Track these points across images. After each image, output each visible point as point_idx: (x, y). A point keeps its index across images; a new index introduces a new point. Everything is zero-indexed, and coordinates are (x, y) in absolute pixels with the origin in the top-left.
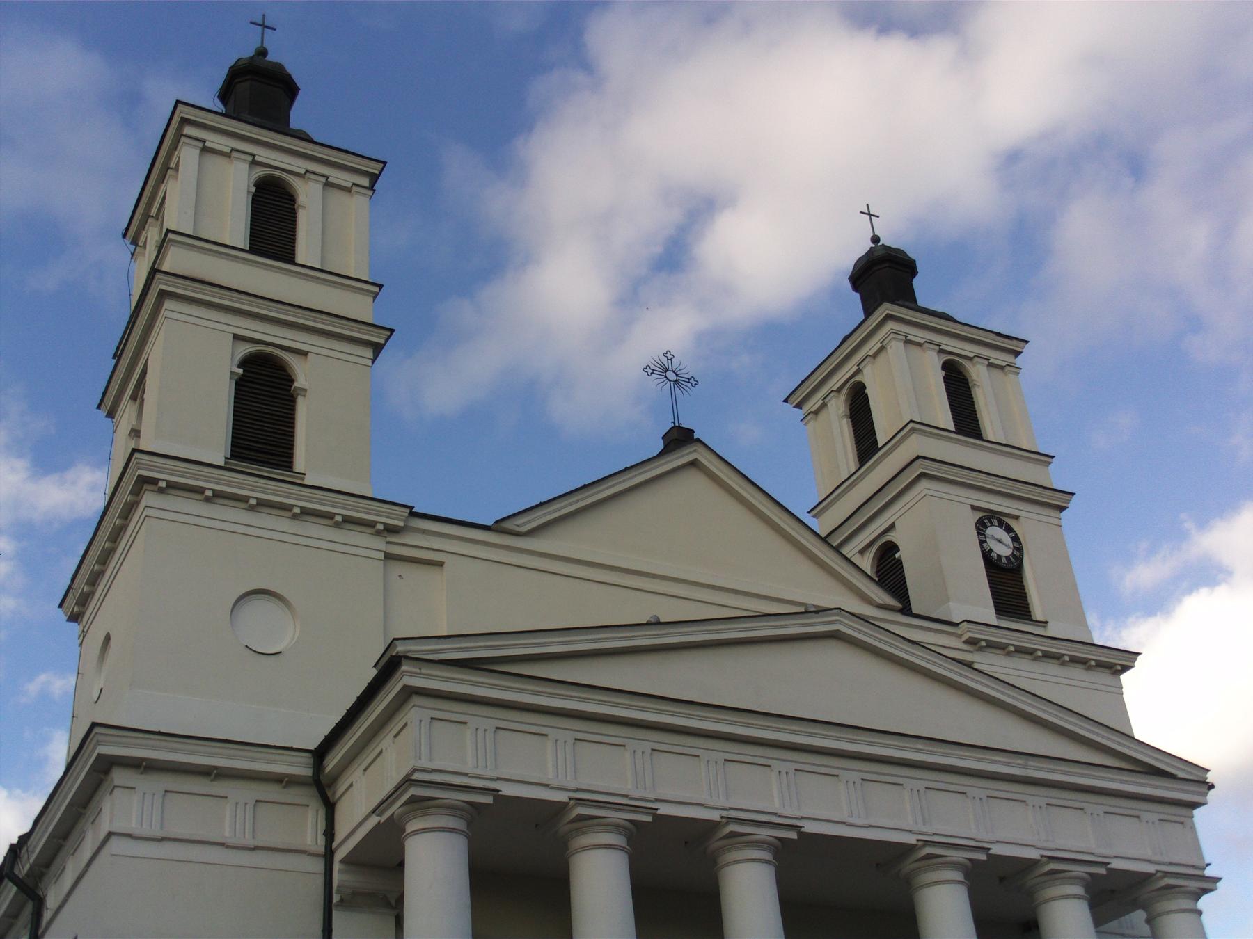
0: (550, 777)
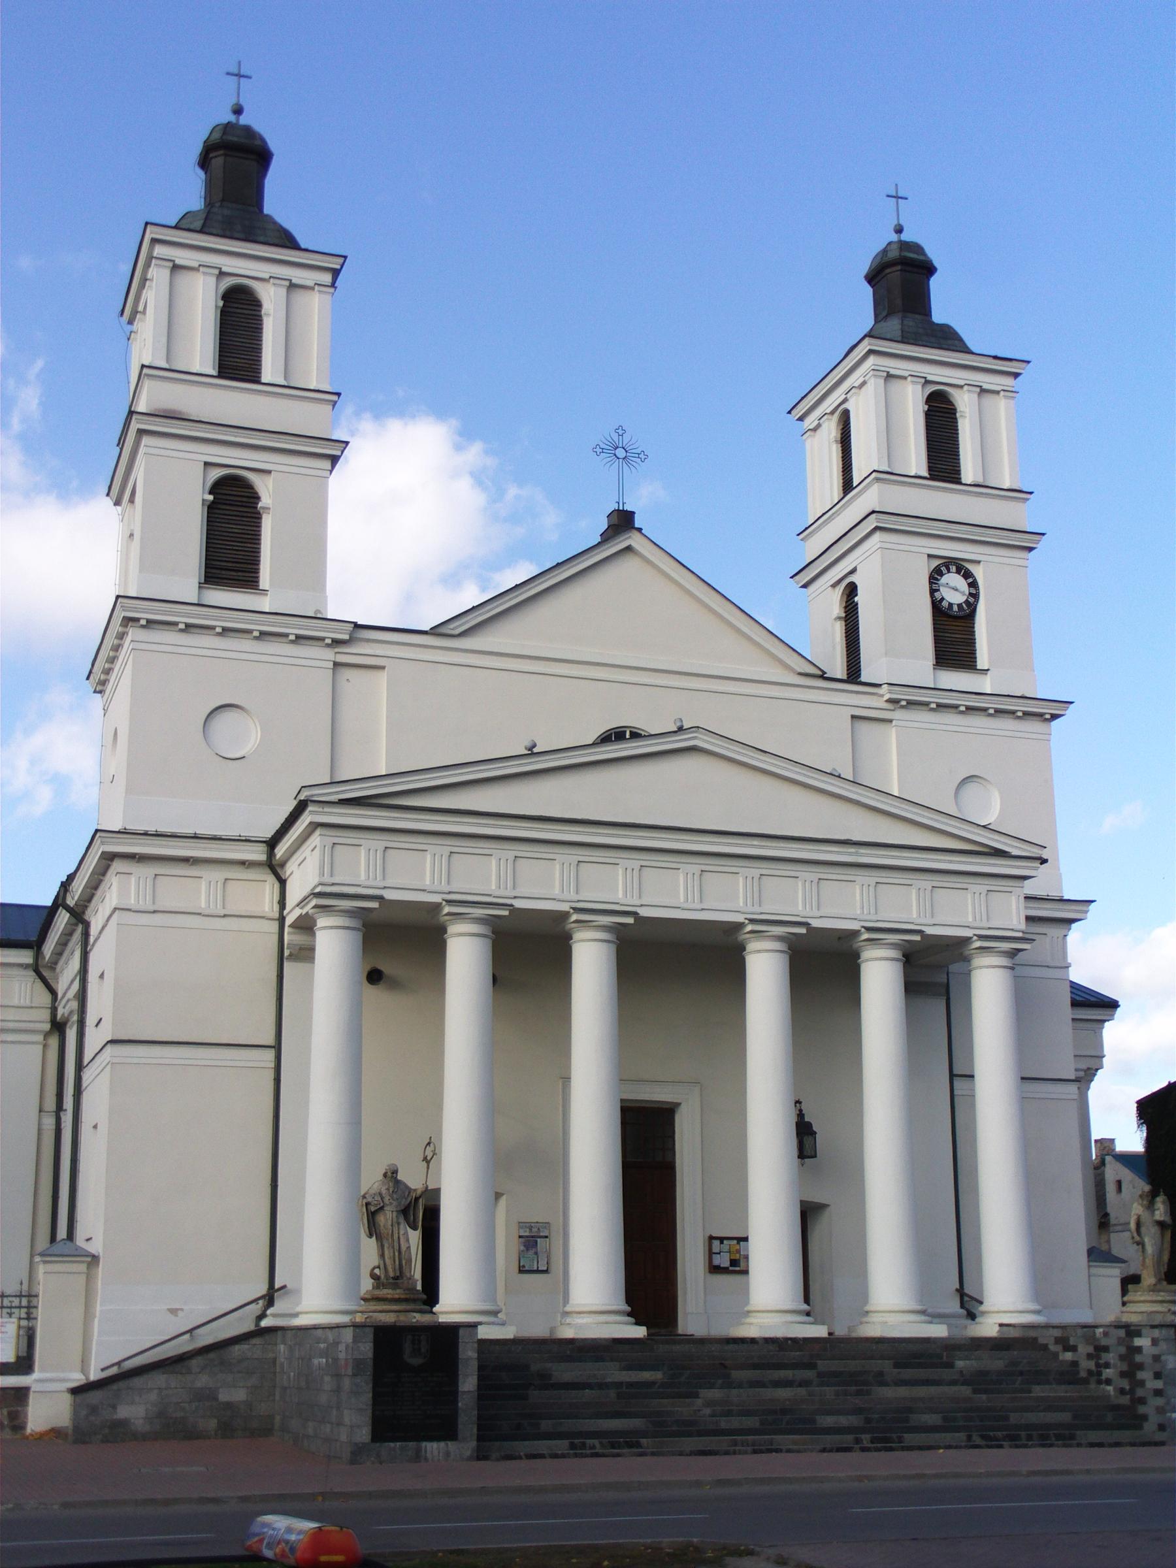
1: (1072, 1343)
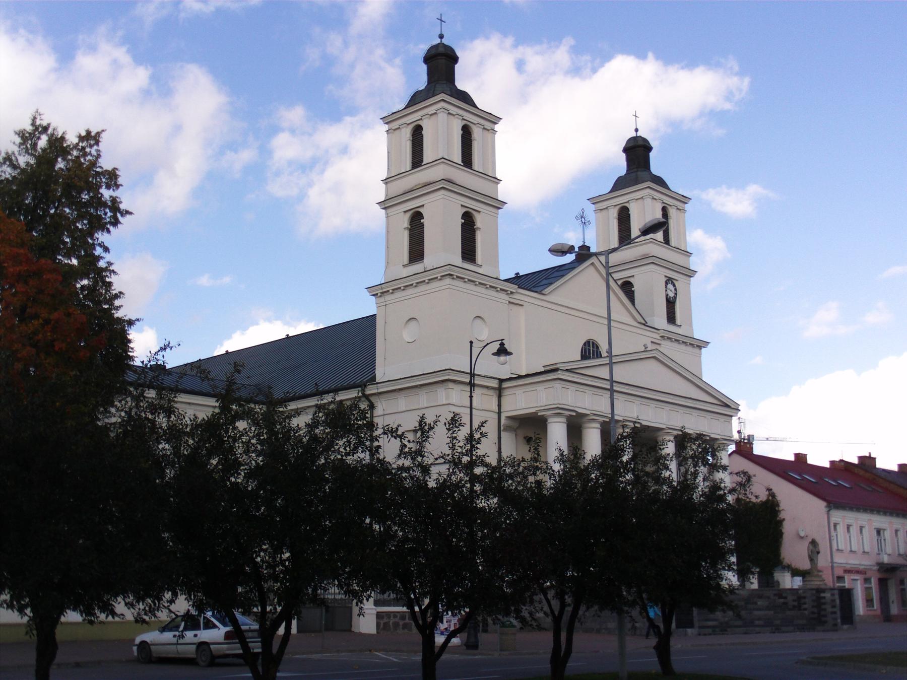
0: (587, 406)
1: (784, 595)
